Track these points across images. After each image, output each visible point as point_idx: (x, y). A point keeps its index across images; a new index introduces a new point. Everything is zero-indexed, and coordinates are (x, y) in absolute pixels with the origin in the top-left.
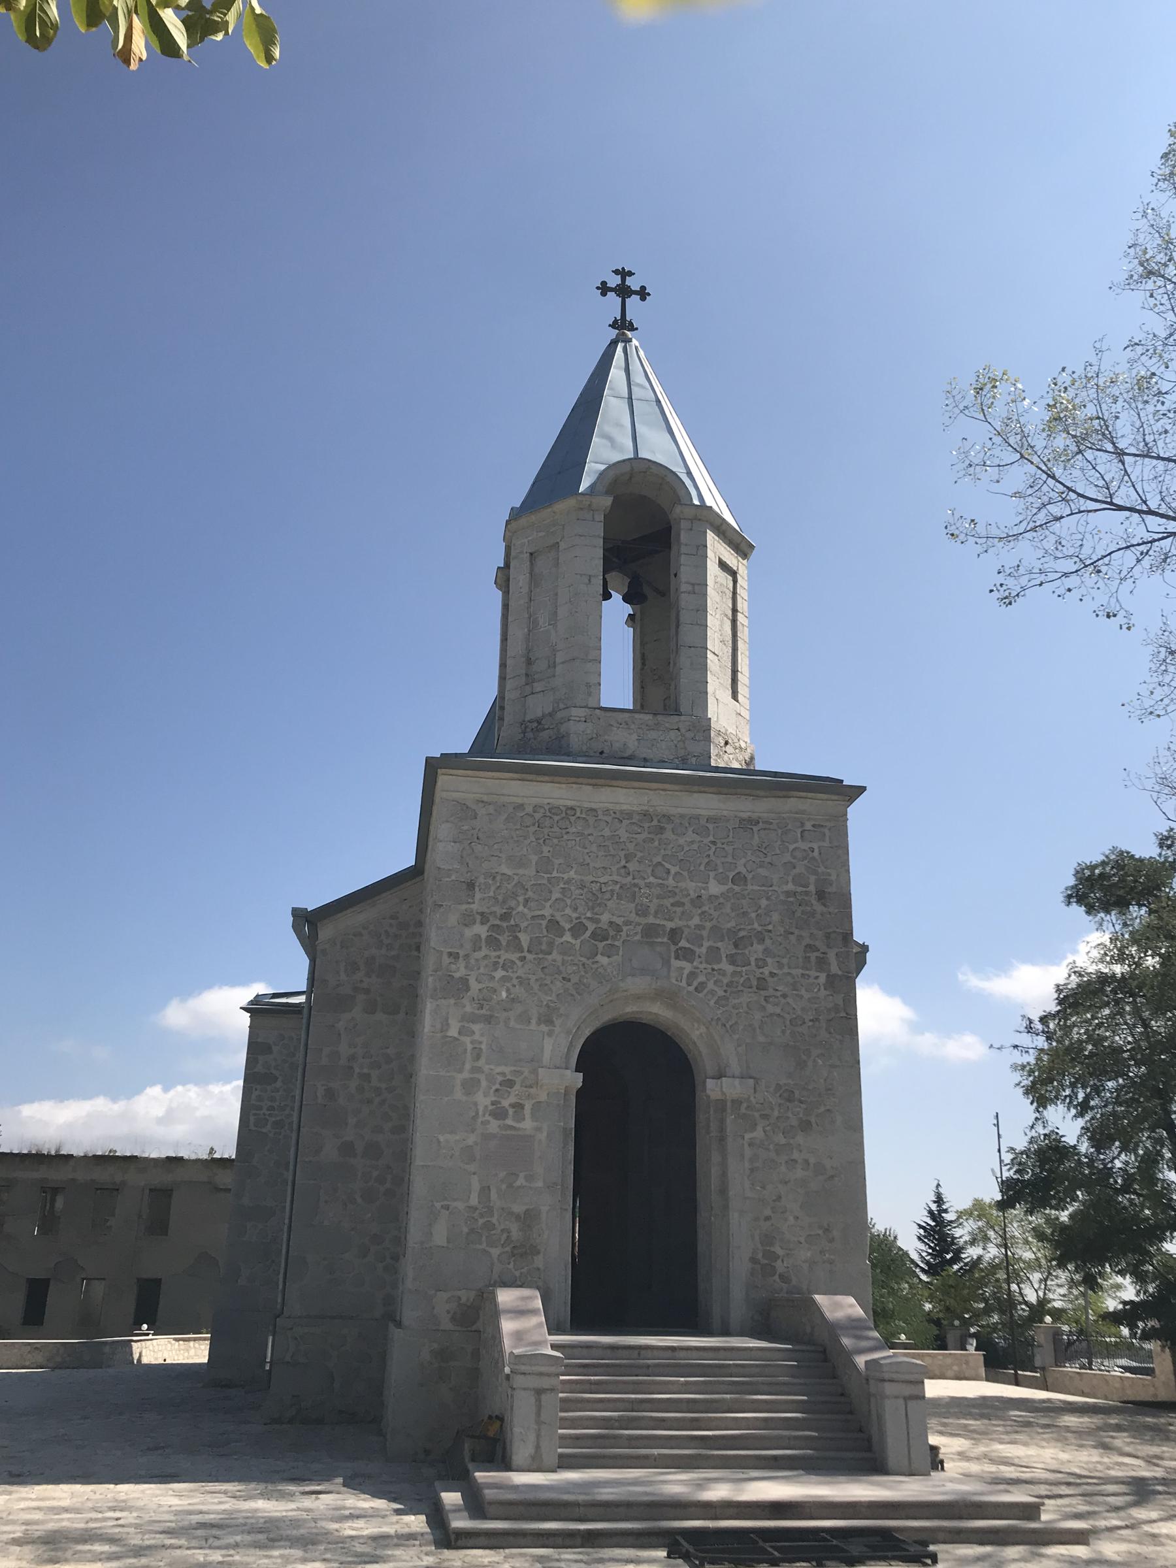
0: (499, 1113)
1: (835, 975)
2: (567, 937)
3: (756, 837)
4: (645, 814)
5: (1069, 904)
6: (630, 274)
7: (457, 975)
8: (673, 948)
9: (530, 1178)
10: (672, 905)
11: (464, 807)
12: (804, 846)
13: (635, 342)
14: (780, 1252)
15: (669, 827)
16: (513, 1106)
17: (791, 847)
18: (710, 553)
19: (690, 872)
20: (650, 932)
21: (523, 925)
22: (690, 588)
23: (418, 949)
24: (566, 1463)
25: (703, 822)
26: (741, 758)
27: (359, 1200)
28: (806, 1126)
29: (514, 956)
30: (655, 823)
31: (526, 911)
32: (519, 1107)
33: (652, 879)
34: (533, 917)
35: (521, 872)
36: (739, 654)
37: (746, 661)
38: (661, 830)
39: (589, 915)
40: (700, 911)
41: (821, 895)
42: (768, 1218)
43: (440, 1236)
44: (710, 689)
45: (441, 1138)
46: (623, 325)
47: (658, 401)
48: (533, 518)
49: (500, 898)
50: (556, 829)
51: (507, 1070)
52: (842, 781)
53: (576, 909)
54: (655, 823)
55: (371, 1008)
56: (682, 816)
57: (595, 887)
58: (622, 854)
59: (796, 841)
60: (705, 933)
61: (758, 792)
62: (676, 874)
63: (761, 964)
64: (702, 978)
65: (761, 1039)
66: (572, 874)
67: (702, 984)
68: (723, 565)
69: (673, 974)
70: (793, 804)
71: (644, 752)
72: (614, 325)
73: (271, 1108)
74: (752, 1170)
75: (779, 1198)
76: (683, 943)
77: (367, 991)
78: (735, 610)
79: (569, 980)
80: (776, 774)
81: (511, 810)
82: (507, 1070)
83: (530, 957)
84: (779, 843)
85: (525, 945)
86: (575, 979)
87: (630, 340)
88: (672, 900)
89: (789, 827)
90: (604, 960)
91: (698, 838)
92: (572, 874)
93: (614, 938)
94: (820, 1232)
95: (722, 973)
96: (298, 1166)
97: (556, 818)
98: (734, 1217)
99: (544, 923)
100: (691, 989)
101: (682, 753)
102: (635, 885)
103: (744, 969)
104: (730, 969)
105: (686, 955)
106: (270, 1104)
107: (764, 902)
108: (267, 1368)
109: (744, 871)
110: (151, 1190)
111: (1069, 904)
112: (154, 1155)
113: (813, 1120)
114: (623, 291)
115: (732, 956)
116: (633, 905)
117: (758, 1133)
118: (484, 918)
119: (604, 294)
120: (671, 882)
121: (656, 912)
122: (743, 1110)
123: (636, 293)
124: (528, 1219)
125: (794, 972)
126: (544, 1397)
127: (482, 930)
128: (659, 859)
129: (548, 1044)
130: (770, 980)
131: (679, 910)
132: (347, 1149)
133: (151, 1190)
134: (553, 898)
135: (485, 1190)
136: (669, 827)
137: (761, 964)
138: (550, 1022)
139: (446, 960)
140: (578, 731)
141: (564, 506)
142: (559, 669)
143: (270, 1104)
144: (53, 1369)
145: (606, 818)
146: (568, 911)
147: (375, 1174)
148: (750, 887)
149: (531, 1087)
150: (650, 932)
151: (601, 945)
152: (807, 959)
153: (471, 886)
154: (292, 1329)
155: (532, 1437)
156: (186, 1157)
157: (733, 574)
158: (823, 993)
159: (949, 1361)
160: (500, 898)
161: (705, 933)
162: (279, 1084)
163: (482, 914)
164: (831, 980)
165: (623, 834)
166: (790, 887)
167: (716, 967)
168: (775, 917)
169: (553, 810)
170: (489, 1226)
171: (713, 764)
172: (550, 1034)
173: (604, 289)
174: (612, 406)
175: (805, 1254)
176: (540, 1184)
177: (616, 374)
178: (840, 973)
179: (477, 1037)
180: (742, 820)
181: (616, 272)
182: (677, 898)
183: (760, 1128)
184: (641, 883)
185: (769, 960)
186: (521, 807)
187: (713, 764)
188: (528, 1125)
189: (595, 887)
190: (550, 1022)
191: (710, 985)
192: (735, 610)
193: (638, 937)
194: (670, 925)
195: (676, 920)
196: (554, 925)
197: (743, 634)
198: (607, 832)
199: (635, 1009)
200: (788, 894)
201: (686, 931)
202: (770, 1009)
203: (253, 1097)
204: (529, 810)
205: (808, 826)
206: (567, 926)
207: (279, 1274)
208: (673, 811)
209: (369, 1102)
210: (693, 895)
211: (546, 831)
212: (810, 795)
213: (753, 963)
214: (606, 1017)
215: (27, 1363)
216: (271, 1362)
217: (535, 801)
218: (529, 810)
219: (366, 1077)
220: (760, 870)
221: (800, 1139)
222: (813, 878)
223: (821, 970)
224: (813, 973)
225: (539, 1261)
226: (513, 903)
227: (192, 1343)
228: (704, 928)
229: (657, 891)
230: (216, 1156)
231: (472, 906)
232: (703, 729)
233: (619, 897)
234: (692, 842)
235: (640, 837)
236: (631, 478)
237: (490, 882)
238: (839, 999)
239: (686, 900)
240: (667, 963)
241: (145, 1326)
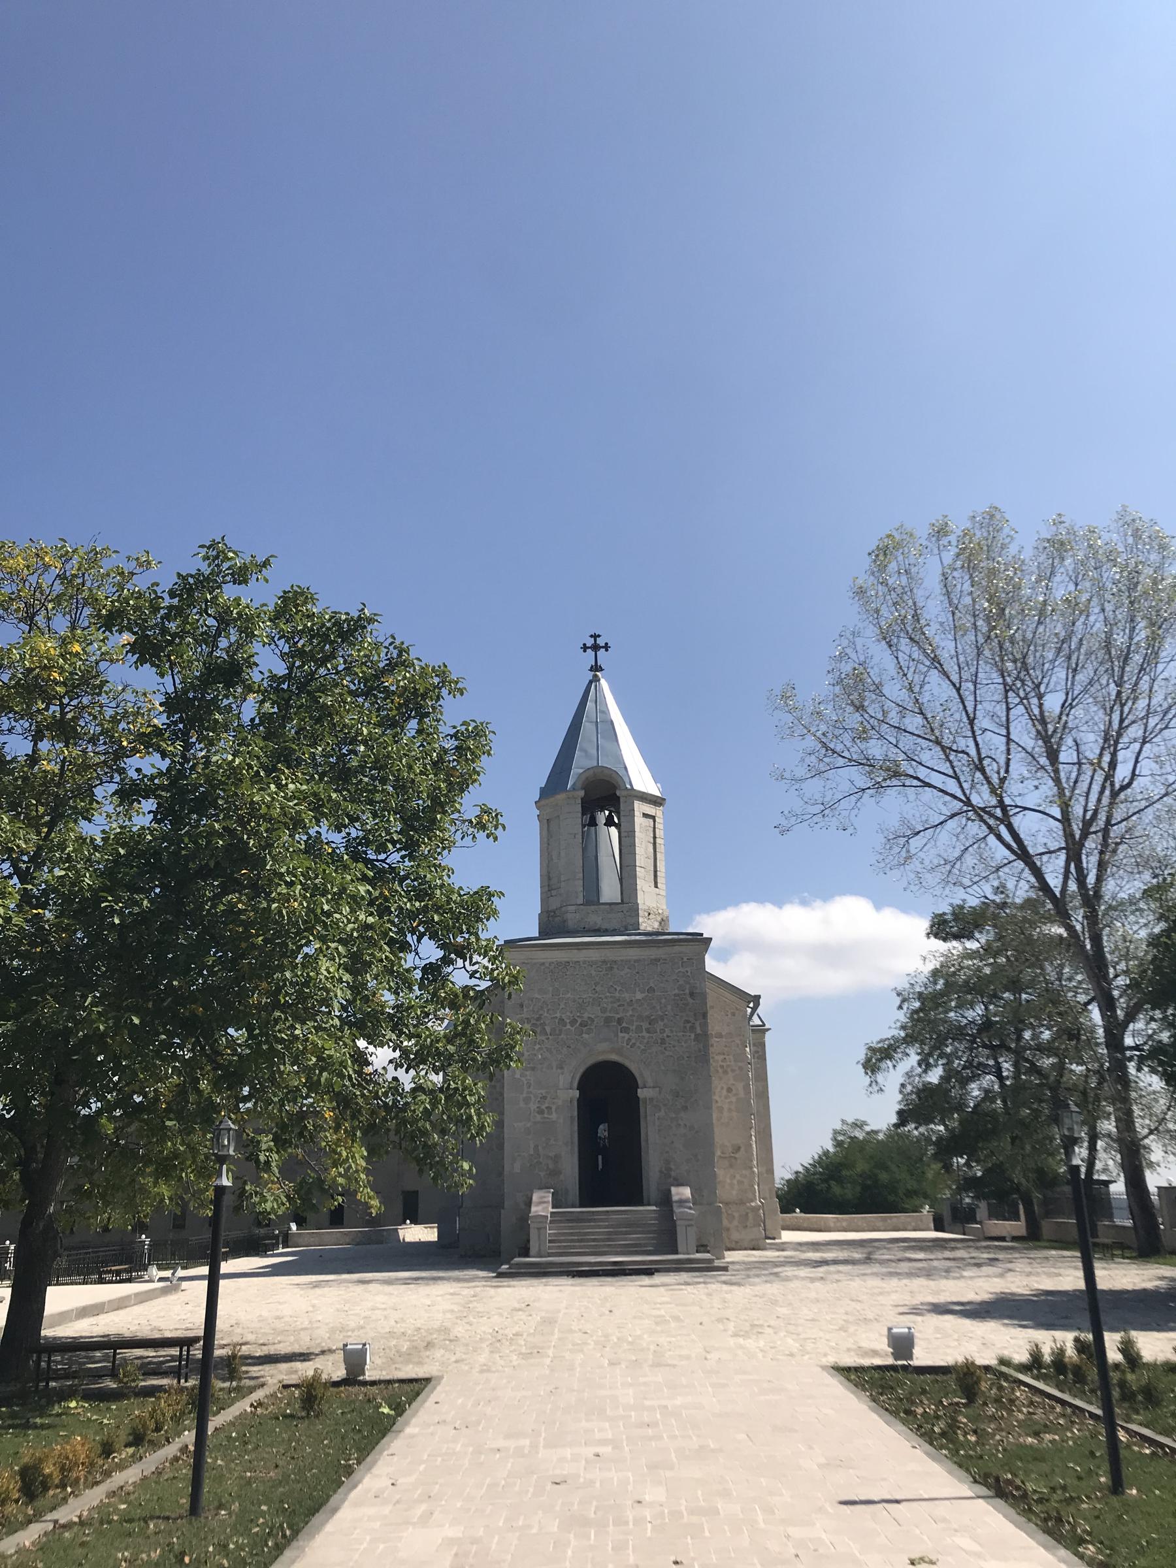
0: (541, 1112)
1: (699, 1034)
2: (568, 1026)
4: (604, 962)
5: (929, 938)
6: (599, 636)
12: (681, 969)
13: (603, 681)
14: (673, 1167)
18: (637, 813)
20: (608, 1020)
21: (547, 1022)
24: (549, 1255)
26: (659, 919)
28: (685, 1108)
29: (543, 1038)
32: (549, 1108)
37: (663, 863)
38: (611, 968)
41: (692, 994)
42: (667, 1152)
43: (517, 1169)
44: (639, 887)
45: (516, 1125)
46: (596, 668)
47: (612, 723)
48: (547, 801)
49: (536, 1010)
51: (543, 1091)
52: (702, 934)
56: (622, 961)
57: (581, 1001)
60: (635, 1019)
63: (662, 1031)
64: (633, 1041)
65: (663, 1068)
66: (569, 995)
67: (634, 1044)
68: (645, 815)
70: (677, 949)
71: (605, 926)
72: (591, 670)
74: (659, 1130)
76: (624, 1025)
78: (655, 837)
80: (669, 934)
82: (543, 1091)
85: (548, 1032)
87: (599, 680)
92: (569, 995)
95: (643, 1037)
98: (651, 1152)
101: (624, 923)
105: (626, 1030)
107: (663, 1001)
109: (652, 985)
111: (929, 938)
114: (596, 648)
117: (662, 1113)
119: (585, 651)
123: (603, 647)
124: (556, 1160)
125: (679, 1034)
129: (561, 1077)
130: (667, 1039)
131: (622, 1008)
135: (536, 1147)
137: (662, 1031)
138: (562, 1068)
140: (572, 917)
141: (561, 797)
142: (563, 884)
144: (358, 1244)
146: (568, 1014)
150: (608, 1020)
151: (584, 1029)
152: (685, 1027)
153: (522, 1006)
157: (653, 818)
158: (693, 1043)
159: (909, 1220)
160: (536, 1010)
161: (635, 1019)
164: (697, 1036)
165: (594, 973)
166: (676, 991)
168: (669, 1007)
169: (559, 964)
171: (642, 927)
173: (585, 648)
174: (587, 727)
177: (590, 705)
180: (651, 960)
181: (591, 636)
184: (603, 996)
186: (543, 964)
188: (554, 1116)
189: (581, 1001)
190: (562, 1068)
191: (638, 1044)
192: (655, 837)
197: (661, 849)
200: (675, 995)
202: (667, 1053)
204: (547, 965)
205: (685, 959)
208: (616, 959)
209: (497, 1099)
214: (591, 1061)
217: (549, 960)
218: (547, 965)
220: (662, 985)
222: (688, 986)
223: (691, 1032)
224: (688, 1034)
225: (562, 1177)
226: (541, 1012)
229: (610, 1000)
232: (635, 910)
240: (617, 1036)
241: (408, 1221)
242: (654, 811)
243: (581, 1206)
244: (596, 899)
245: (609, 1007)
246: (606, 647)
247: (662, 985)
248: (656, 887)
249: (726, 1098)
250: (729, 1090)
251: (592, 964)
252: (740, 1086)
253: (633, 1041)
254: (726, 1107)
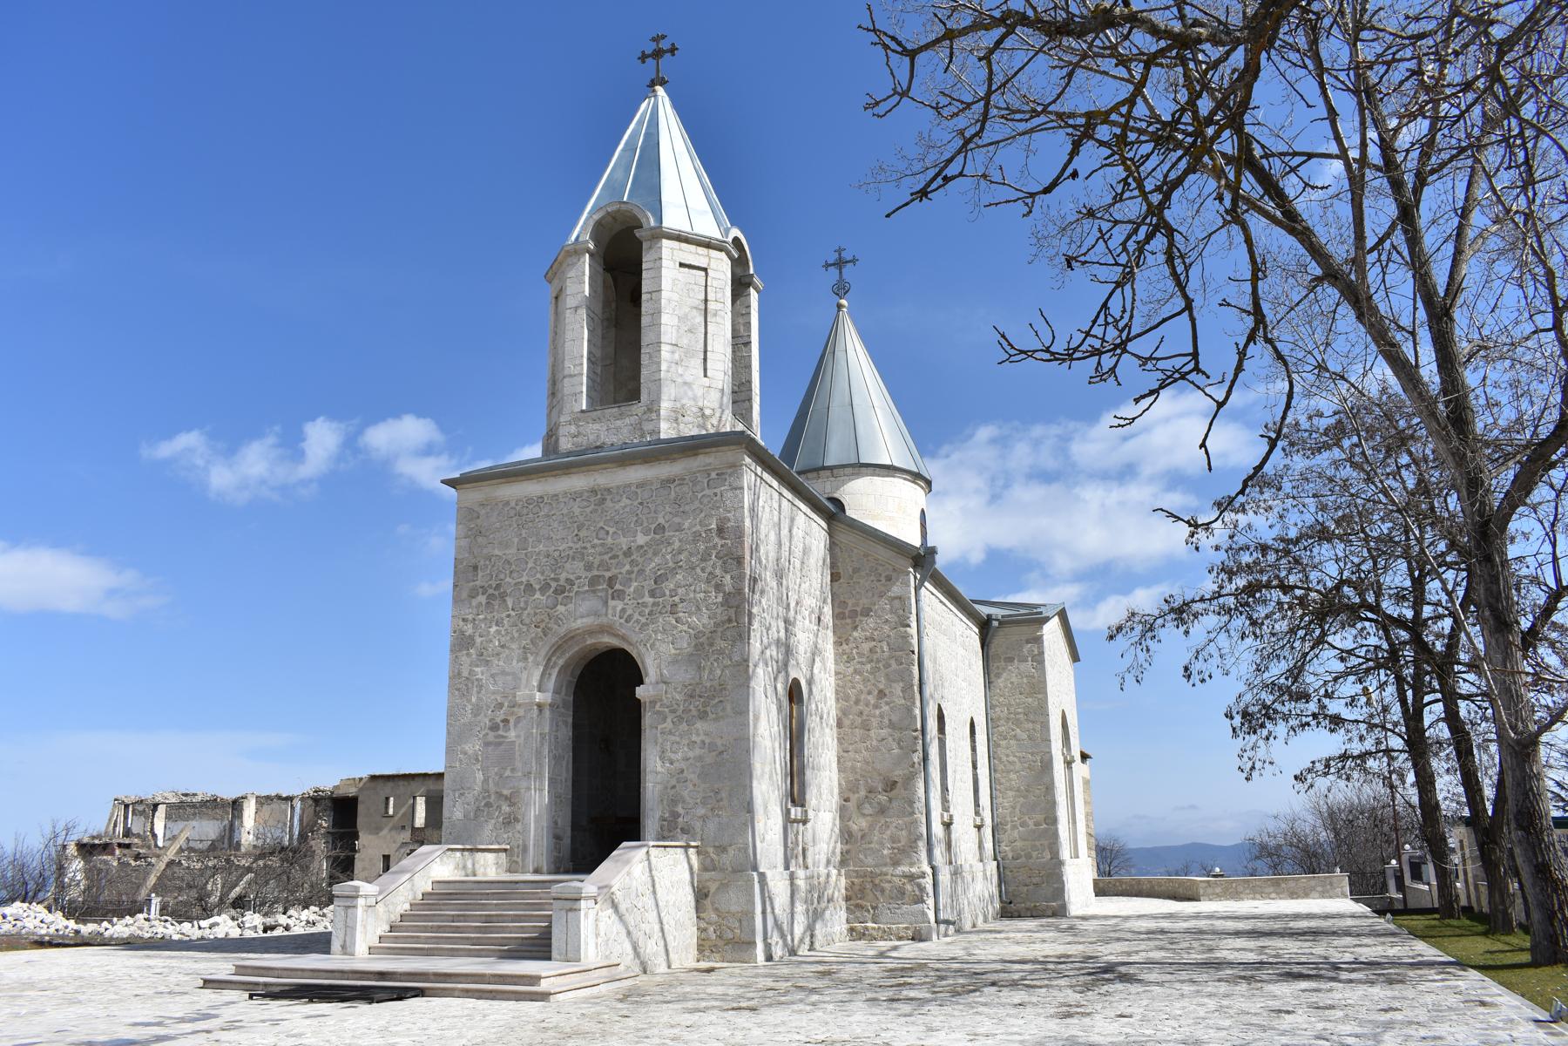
2: (538, 595)
3: (673, 492)
4: (594, 491)
6: (663, 37)
7: (467, 634)
8: (610, 591)
9: (513, 770)
10: (610, 558)
11: (470, 510)
15: (609, 497)
16: (503, 721)
17: (700, 496)
19: (623, 530)
22: (649, 296)
25: (633, 488)
28: (703, 715)
30: (599, 496)
31: (510, 580)
32: (506, 721)
33: (596, 541)
34: (515, 584)
35: (507, 552)
36: (709, 335)
39: (552, 576)
40: (629, 559)
42: (674, 787)
50: (531, 515)
53: (543, 573)
54: (599, 496)
56: (618, 487)
57: (557, 553)
58: (575, 525)
59: (703, 490)
60: (633, 576)
61: (676, 456)
62: (615, 533)
63: (673, 593)
64: (629, 612)
67: (630, 617)
69: (610, 611)
75: (682, 771)
76: (618, 587)
79: (538, 627)
81: (500, 506)
83: (513, 613)
84: (691, 493)
86: (543, 625)
88: (610, 555)
89: (699, 479)
90: (561, 608)
91: (628, 502)
93: (569, 591)
94: (712, 794)
95: (644, 605)
97: (531, 507)
99: (522, 587)
100: (622, 621)
102: (585, 548)
103: (661, 600)
104: (651, 600)
105: (618, 595)
113: (708, 709)
115: (652, 590)
116: (582, 564)
117: (668, 725)
118: (484, 590)
120: (610, 540)
121: (599, 566)
122: (657, 708)
126: (350, 911)
127: (482, 599)
128: (601, 524)
134: (530, 565)
135: (486, 781)
136: (609, 497)
137: (673, 593)
138: (526, 659)
139: (461, 623)
145: (566, 500)
146: (539, 576)
148: (667, 534)
149: (514, 707)
150: (594, 581)
151: (560, 598)
153: (475, 568)
155: (342, 936)
157: (705, 270)
163: (482, 587)
164: (727, 596)
165: (577, 511)
167: (640, 601)
169: (529, 501)
170: (488, 805)
172: (525, 669)
173: (643, 58)
175: (701, 811)
176: (520, 774)
178: (733, 591)
179: (480, 676)
181: (654, 39)
182: (613, 553)
183: (669, 720)
184: (588, 545)
185: (680, 591)
186: (507, 503)
187: (663, 436)
191: (636, 616)
192: (706, 300)
193: (586, 588)
194: (608, 574)
195: (613, 570)
196: (529, 586)
198: (565, 511)
199: (593, 641)
201: (620, 576)
204: (513, 504)
205: (713, 475)
206: (537, 587)
207: (499, 844)
210: (625, 548)
211: (524, 518)
212: (714, 449)
213: (668, 593)
220: (677, 520)
221: (699, 725)
226: (502, 576)
228: (633, 572)
231: (477, 583)
233: (573, 559)
234: (625, 507)
235: (588, 510)
236: (614, 218)
237: (487, 562)
238: (732, 611)
239: (620, 553)
240: (606, 603)
242: (707, 260)
243: (550, 873)
245: (596, 563)
246: (673, 50)
247: (677, 520)
248: (705, 376)
249: (876, 707)
250: (882, 694)
251: (575, 496)
252: (897, 688)
253: (629, 612)
254: (874, 722)
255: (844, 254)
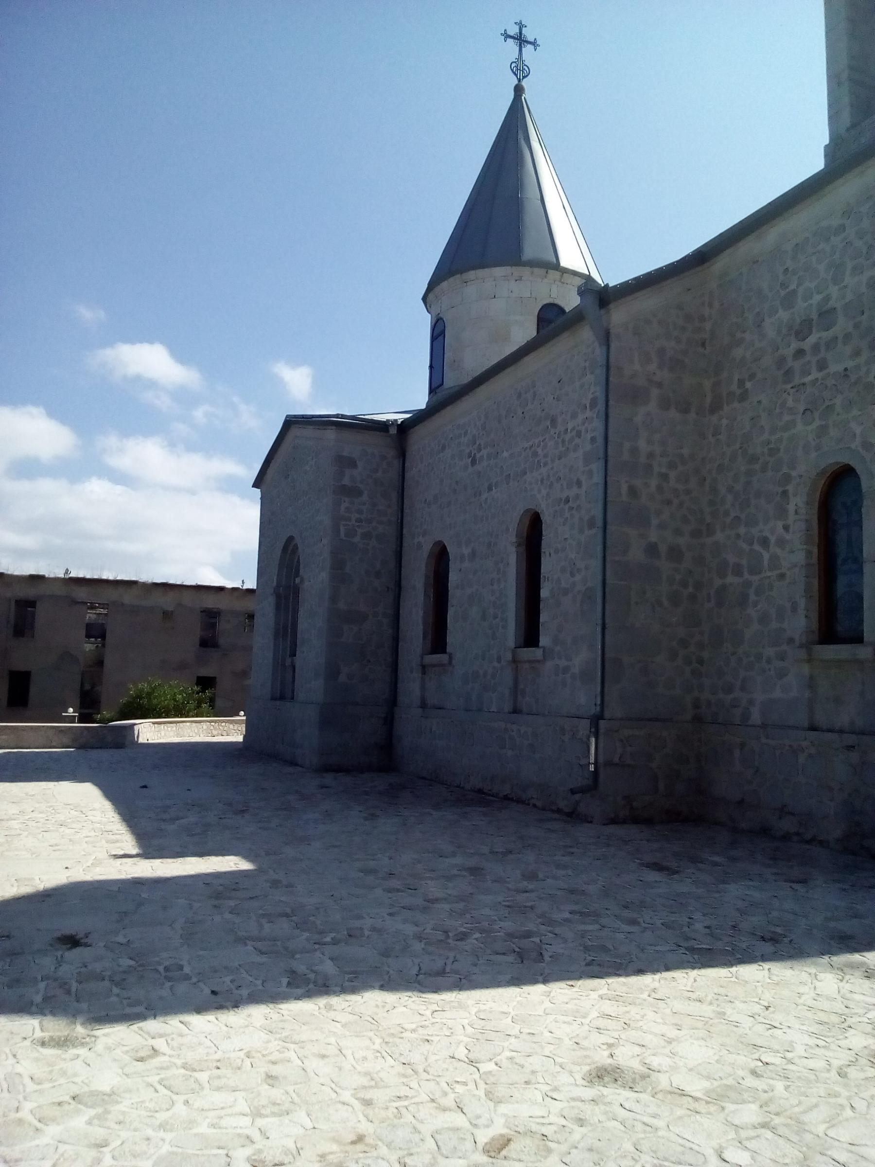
23: (703, 345)
27: (666, 603)
55: (665, 404)
73: (359, 520)
77: (660, 385)
96: (608, 566)
106: (357, 516)
108: (592, 768)
110: (16, 601)
112: (16, 573)
132: (652, 550)
133: (16, 601)
143: (357, 516)
147: (678, 577)
154: (617, 731)
156: (47, 576)
162: (365, 498)
203: (343, 508)
215: (54, 744)
216: (596, 763)
219: (664, 477)
227: (162, 726)
230: (73, 575)
244: (554, 260)
255: (524, 31)
